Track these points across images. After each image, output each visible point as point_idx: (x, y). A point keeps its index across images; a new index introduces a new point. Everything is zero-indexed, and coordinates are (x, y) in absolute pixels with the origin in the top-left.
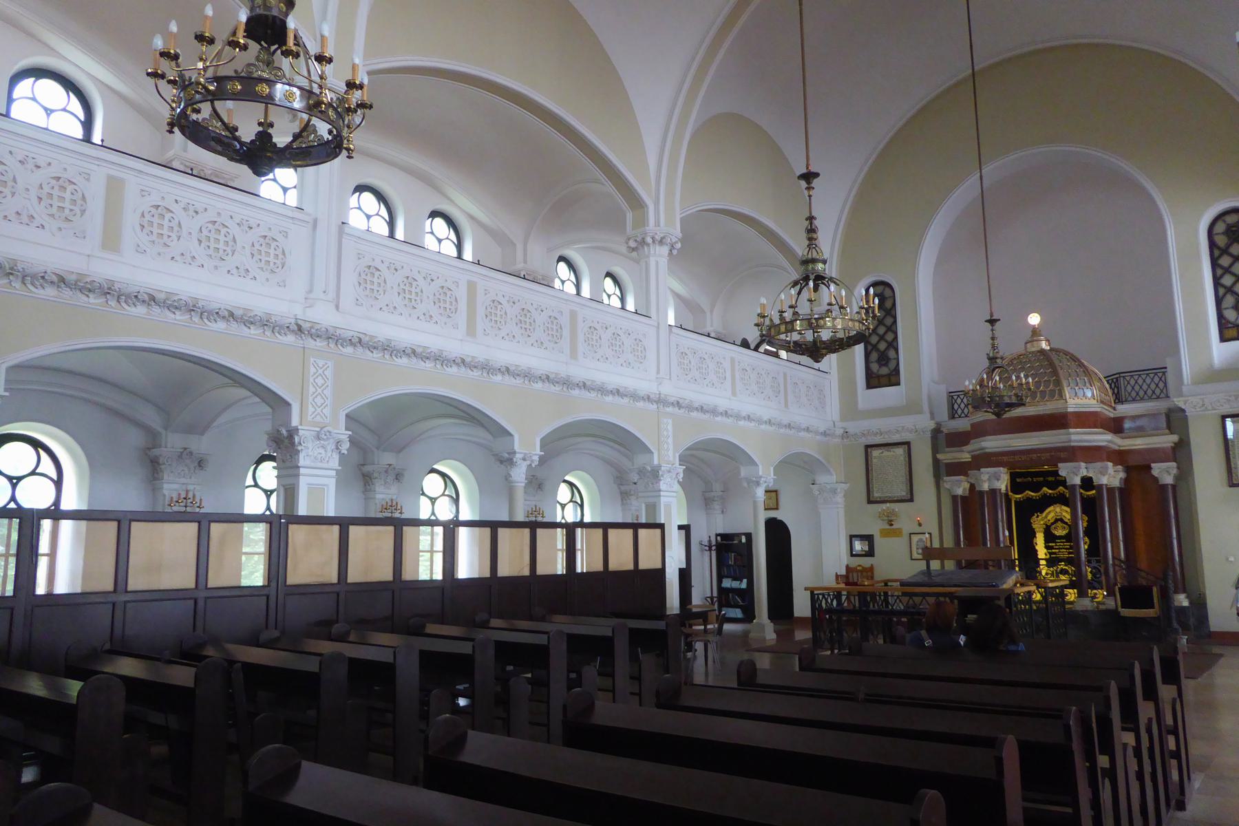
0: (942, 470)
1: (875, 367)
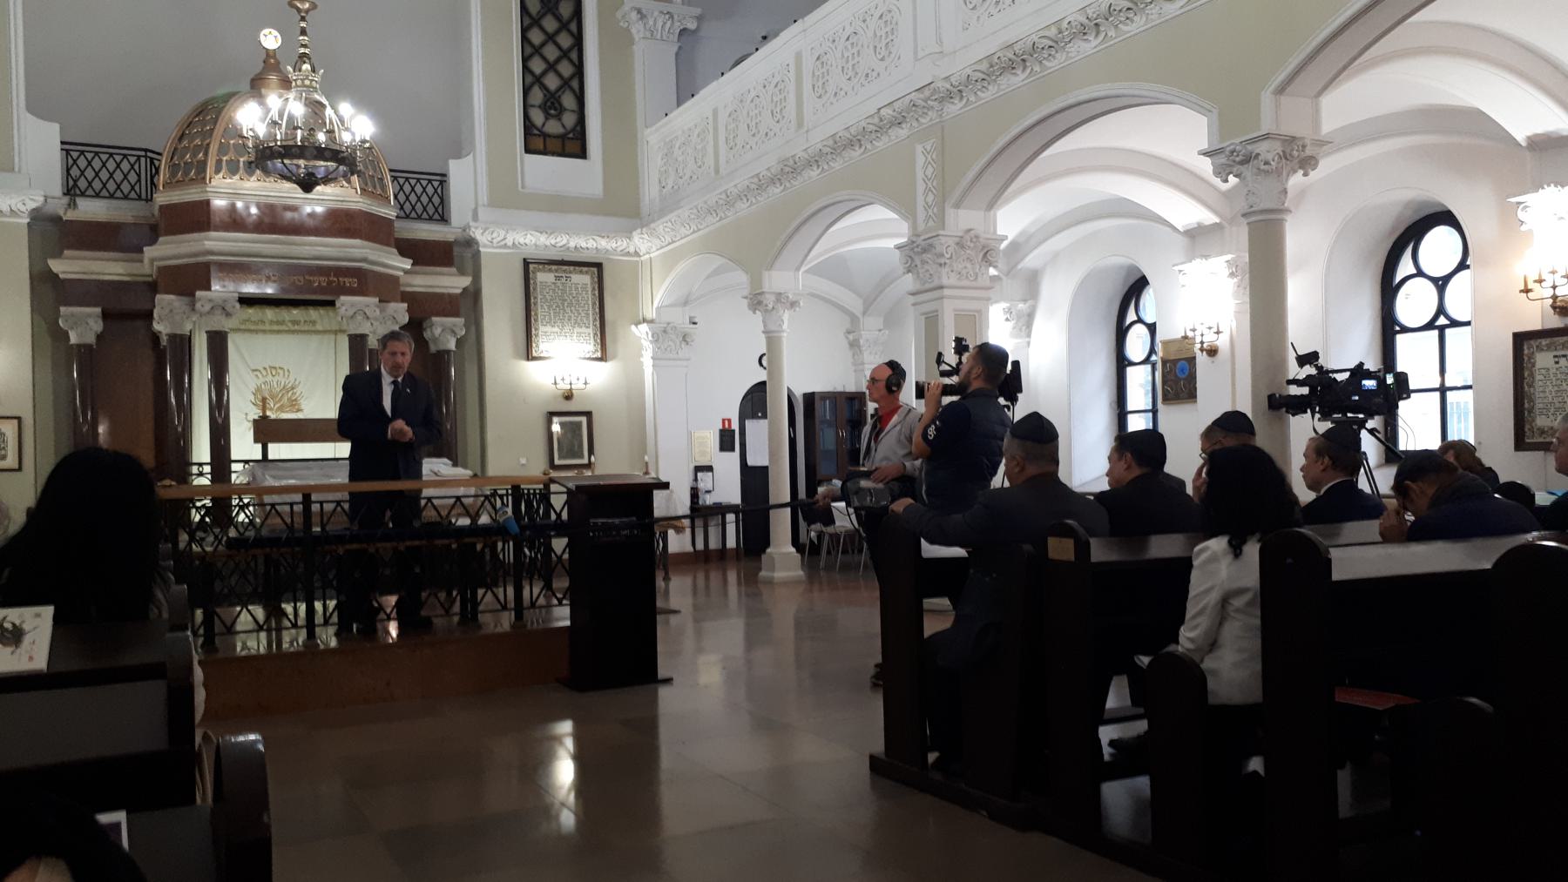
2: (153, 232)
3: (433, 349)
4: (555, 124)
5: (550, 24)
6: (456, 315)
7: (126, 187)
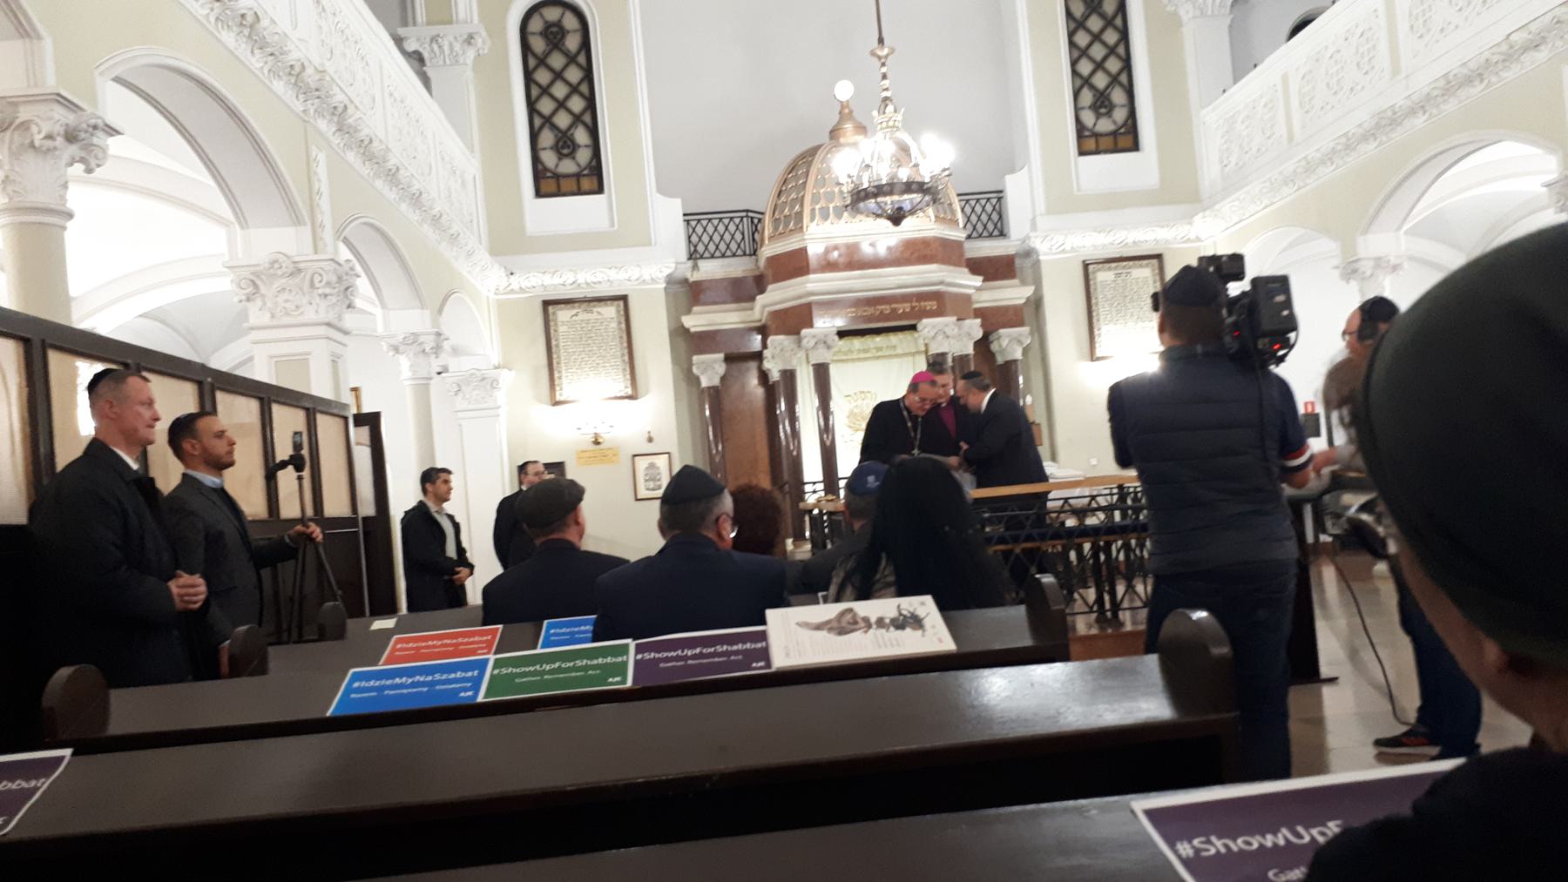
0: (690, 343)
1: (549, 158)
2: (760, 283)
3: (1000, 360)
4: (1107, 123)
5: (1095, 23)
6: (1021, 324)
7: (733, 246)
